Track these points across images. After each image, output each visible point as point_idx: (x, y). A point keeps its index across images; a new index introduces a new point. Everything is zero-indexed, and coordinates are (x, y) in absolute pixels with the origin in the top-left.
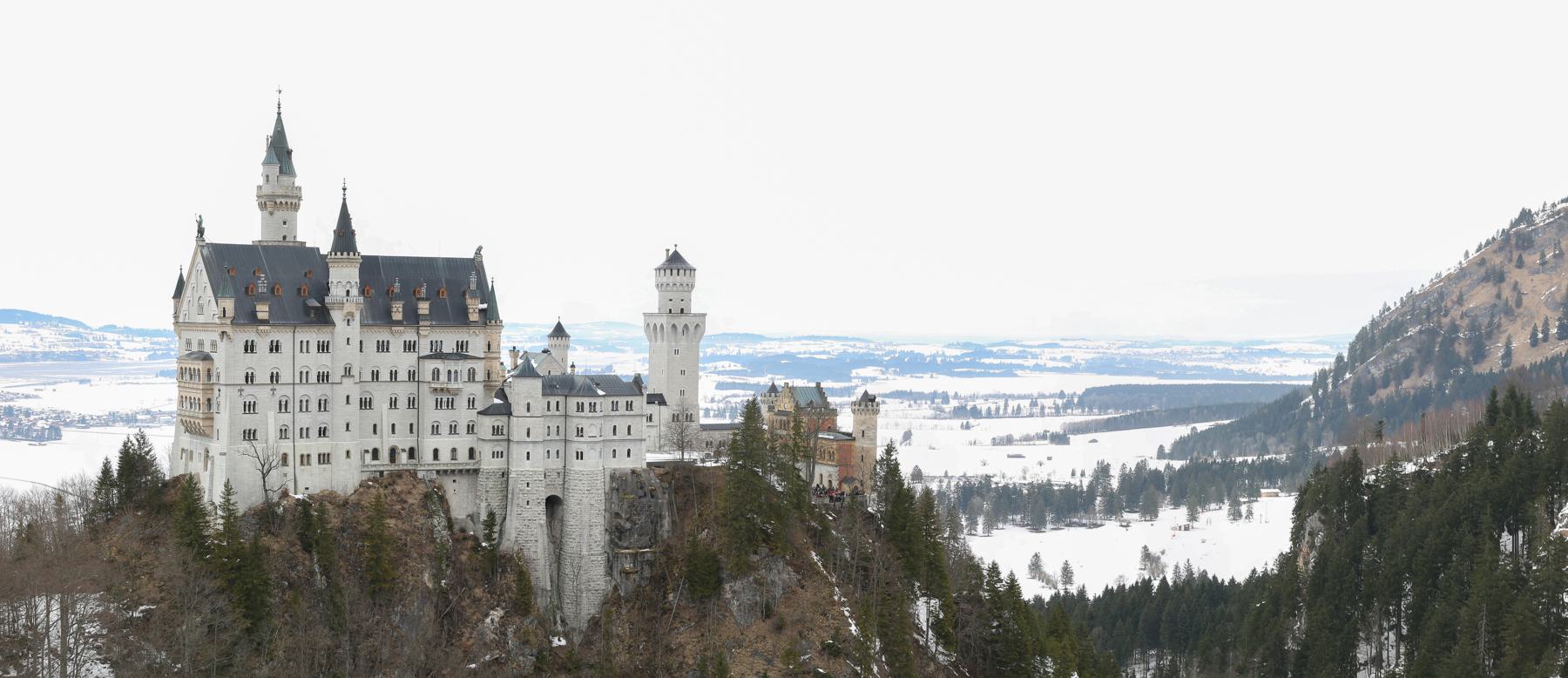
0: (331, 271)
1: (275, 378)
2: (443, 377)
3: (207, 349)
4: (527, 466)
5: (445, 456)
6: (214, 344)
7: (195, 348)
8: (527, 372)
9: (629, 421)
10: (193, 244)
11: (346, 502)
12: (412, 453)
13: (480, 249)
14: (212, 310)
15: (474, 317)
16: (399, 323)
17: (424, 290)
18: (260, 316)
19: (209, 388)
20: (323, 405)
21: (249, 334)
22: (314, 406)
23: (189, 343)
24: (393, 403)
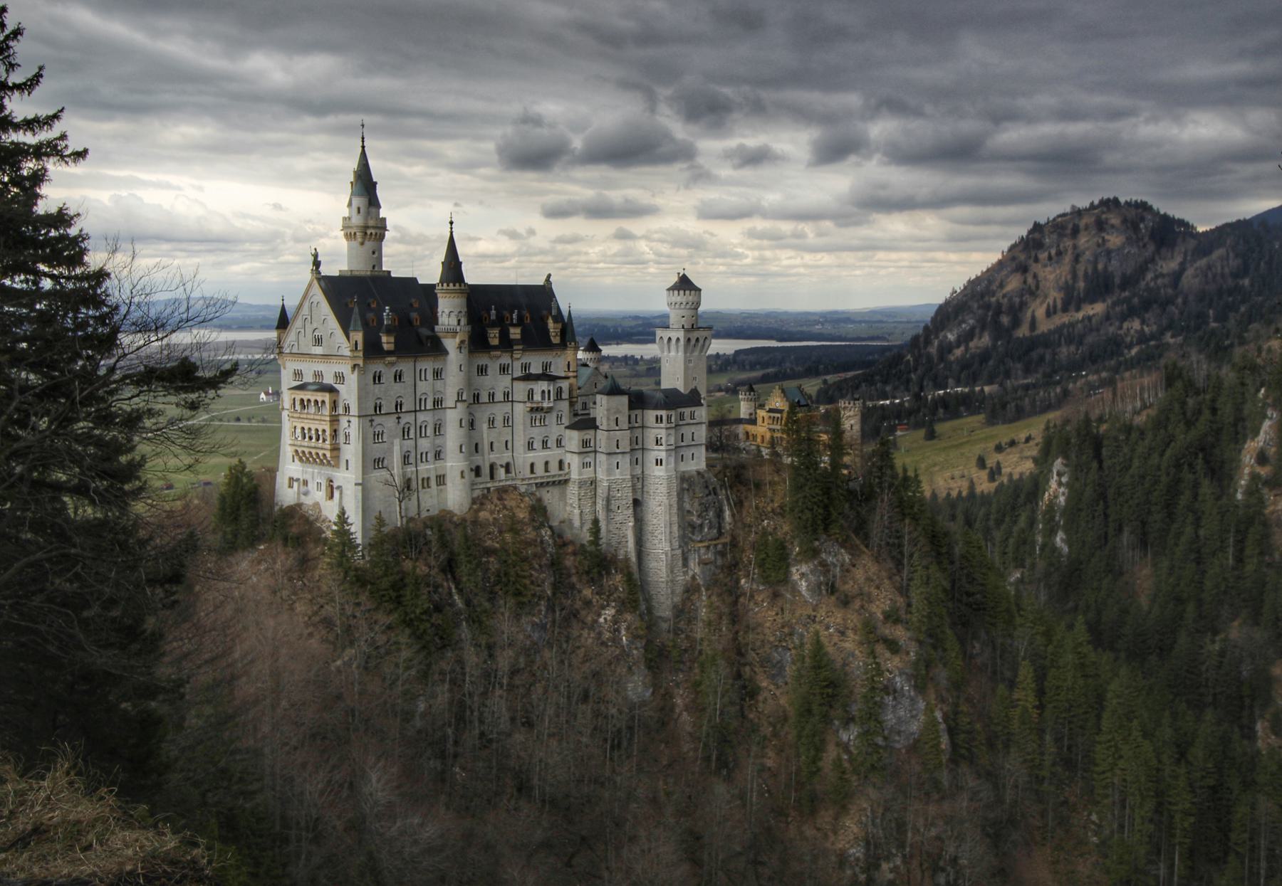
0: (441, 301)
1: (399, 405)
2: (537, 397)
3: (329, 380)
4: (617, 475)
5: (539, 470)
6: (340, 377)
7: (309, 378)
8: (614, 391)
9: (693, 429)
10: (306, 274)
11: (464, 520)
12: (507, 468)
13: (549, 276)
14: (339, 341)
15: (556, 340)
16: (495, 348)
17: (515, 316)
18: (386, 347)
19: (334, 420)
20: (438, 429)
21: (377, 366)
22: (430, 431)
23: (298, 374)
24: (491, 422)
